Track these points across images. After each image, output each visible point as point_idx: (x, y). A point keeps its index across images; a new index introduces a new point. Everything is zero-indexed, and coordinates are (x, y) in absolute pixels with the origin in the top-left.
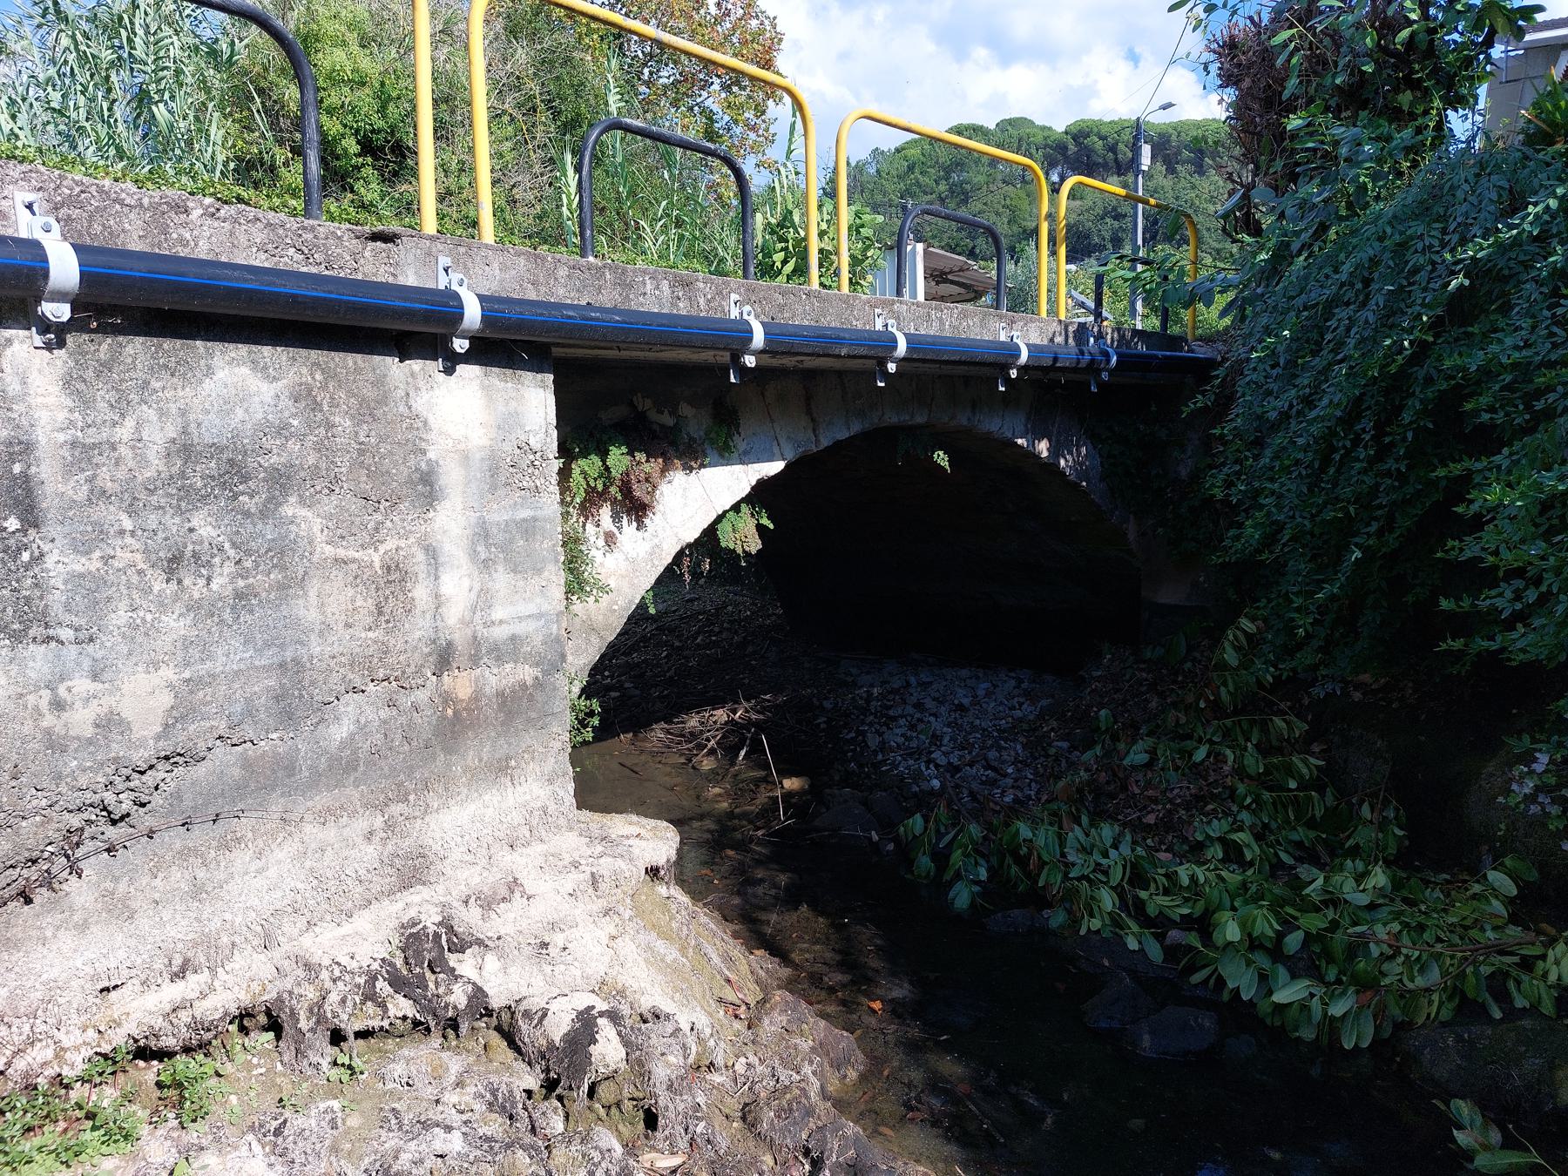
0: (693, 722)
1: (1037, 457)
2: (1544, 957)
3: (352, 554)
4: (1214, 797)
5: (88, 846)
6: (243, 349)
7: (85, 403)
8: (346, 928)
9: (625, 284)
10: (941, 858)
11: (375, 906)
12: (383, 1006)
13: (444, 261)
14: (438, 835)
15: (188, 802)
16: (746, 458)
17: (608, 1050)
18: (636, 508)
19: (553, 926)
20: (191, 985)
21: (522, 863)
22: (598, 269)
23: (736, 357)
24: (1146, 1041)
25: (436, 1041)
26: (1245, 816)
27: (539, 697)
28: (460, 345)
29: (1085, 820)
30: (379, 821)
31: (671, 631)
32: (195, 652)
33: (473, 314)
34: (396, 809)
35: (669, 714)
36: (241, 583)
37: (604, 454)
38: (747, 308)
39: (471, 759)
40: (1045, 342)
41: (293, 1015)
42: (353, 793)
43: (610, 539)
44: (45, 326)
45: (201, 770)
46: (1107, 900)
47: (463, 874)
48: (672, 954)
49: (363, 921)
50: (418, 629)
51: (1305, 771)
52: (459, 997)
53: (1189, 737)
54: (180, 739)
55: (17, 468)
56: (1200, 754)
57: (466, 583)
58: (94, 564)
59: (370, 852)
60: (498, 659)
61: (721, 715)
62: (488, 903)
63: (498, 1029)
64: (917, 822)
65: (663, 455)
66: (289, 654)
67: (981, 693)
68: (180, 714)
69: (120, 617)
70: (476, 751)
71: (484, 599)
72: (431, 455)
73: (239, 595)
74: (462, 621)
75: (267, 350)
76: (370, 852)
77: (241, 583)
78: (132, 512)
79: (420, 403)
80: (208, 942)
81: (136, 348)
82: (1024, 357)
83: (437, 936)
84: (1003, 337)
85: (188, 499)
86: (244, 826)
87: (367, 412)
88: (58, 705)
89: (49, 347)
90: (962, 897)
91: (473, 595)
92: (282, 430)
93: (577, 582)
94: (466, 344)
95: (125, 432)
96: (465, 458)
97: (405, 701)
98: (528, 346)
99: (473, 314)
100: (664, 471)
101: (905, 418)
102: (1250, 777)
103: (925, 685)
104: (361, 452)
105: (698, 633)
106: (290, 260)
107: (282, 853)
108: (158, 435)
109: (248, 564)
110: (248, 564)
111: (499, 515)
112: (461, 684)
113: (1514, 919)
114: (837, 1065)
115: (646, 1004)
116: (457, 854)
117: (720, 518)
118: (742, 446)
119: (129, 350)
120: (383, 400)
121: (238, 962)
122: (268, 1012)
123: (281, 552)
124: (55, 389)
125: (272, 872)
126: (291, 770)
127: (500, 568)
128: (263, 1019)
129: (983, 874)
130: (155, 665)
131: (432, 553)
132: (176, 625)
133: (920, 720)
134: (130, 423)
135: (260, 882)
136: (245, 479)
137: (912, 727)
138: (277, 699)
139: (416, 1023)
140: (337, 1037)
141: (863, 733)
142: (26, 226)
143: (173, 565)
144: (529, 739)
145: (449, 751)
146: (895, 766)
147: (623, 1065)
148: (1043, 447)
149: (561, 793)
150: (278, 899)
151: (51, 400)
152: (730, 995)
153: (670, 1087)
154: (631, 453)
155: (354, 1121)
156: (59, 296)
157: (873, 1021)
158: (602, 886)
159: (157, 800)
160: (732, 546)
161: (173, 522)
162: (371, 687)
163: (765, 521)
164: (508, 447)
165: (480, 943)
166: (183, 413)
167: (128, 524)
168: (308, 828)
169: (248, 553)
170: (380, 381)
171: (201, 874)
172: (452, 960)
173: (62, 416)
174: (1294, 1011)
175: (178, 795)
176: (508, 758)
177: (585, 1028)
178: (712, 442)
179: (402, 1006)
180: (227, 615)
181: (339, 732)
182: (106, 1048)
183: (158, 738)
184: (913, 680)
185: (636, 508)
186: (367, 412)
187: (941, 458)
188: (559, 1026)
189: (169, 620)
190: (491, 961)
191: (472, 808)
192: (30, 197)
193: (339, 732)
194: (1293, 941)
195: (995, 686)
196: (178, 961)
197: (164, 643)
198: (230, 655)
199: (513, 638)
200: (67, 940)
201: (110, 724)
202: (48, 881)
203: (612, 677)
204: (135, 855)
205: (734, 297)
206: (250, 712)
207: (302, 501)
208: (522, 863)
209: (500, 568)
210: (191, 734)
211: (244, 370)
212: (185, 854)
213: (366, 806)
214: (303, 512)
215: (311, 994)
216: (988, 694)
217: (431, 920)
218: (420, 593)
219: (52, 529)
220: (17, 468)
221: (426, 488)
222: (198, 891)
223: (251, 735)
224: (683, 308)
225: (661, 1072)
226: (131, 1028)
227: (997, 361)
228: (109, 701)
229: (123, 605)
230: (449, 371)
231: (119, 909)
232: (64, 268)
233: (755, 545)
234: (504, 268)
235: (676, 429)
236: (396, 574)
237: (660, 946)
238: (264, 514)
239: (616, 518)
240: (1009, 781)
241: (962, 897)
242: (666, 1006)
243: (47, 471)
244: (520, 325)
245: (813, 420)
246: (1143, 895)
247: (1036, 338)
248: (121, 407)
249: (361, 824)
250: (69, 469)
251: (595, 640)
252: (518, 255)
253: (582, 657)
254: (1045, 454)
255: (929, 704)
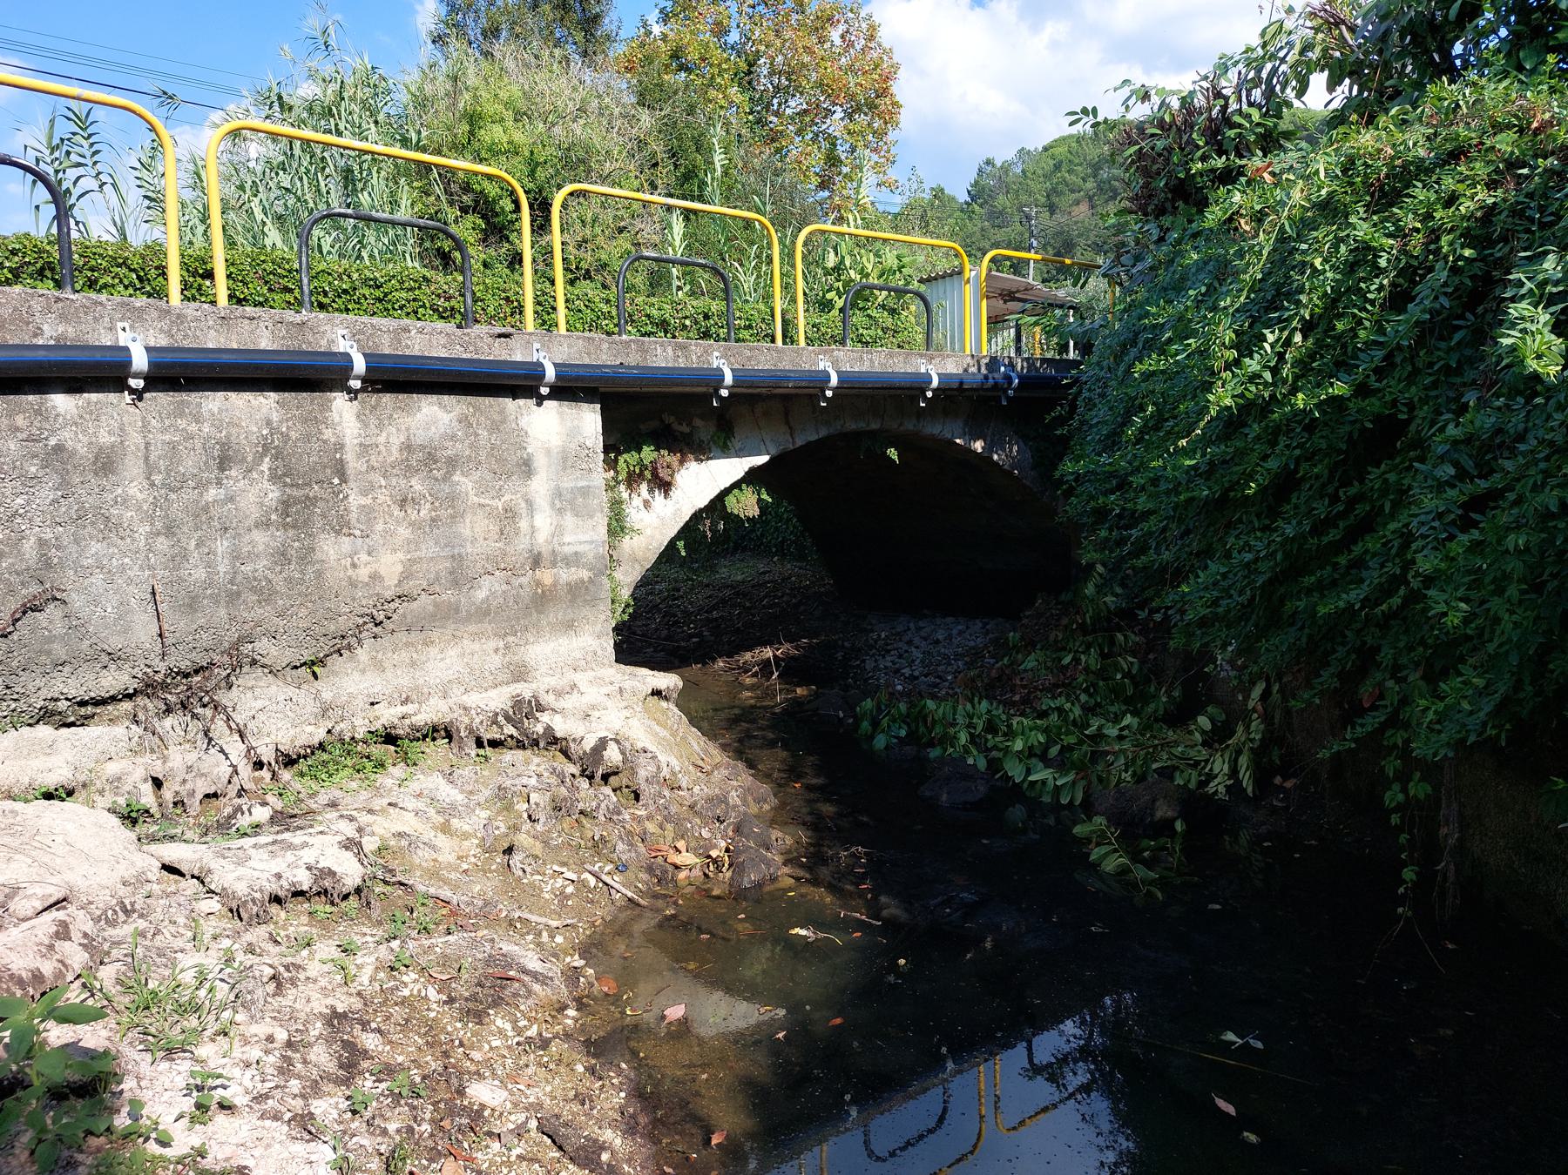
0: (748, 656)
1: (975, 452)
2: (1207, 761)
3: (487, 502)
4: (1064, 685)
5: (365, 634)
6: (435, 397)
7: (366, 425)
8: (484, 695)
9: (643, 350)
10: (875, 724)
11: (499, 688)
12: (501, 727)
13: (537, 345)
14: (533, 657)
15: (409, 620)
16: (726, 451)
17: (613, 755)
18: (664, 486)
19: (593, 707)
20: (409, 709)
21: (581, 678)
22: (626, 342)
23: (717, 390)
24: (944, 797)
25: (528, 752)
26: (1084, 698)
27: (592, 588)
28: (544, 391)
29: (976, 699)
30: (501, 644)
31: (745, 595)
32: (412, 546)
33: (550, 374)
34: (510, 639)
35: (732, 651)
36: (434, 514)
37: (639, 451)
38: (723, 361)
39: (551, 617)
40: (961, 371)
41: (458, 730)
42: (488, 627)
43: (647, 504)
44: (350, 391)
45: (415, 605)
46: (963, 738)
47: (548, 679)
48: (664, 733)
49: (493, 693)
50: (522, 544)
51: (1125, 666)
52: (540, 729)
53: (1064, 649)
54: (404, 589)
55: (338, 456)
56: (1067, 660)
57: (549, 520)
58: (369, 501)
59: (497, 660)
60: (567, 564)
61: (768, 653)
62: (559, 694)
63: (561, 751)
64: (868, 704)
65: (680, 451)
66: (456, 552)
67: (955, 632)
68: (406, 576)
69: (379, 527)
70: (555, 614)
71: (559, 530)
72: (529, 450)
73: (433, 520)
74: (546, 541)
75: (446, 397)
76: (497, 660)
77: (434, 514)
78: (385, 477)
79: (523, 422)
80: (416, 688)
81: (387, 399)
82: (935, 383)
83: (530, 702)
84: (923, 370)
85: (410, 471)
86: (435, 635)
87: (495, 427)
88: (354, 566)
89: (351, 400)
90: (880, 742)
91: (553, 527)
92: (453, 437)
93: (617, 526)
94: (548, 390)
95: (382, 439)
96: (548, 452)
97: (516, 582)
98: (584, 389)
99: (550, 374)
100: (682, 462)
101: (862, 425)
102: (1092, 672)
103: (919, 629)
104: (492, 449)
105: (765, 597)
106: (458, 352)
107: (452, 652)
108: (397, 440)
109: (437, 504)
110: (437, 504)
111: (568, 483)
112: (546, 576)
113: (1204, 744)
114: (758, 801)
115: (639, 745)
116: (543, 669)
117: (726, 492)
118: (738, 445)
119: (384, 400)
120: (504, 421)
121: (432, 701)
122: (446, 729)
123: (452, 499)
124: (354, 419)
125: (448, 661)
126: (457, 611)
127: (568, 514)
128: (443, 733)
129: (903, 733)
130: (395, 551)
131: (530, 503)
132: (404, 532)
133: (906, 651)
134: (384, 434)
135: (441, 665)
136: (436, 462)
137: (900, 656)
138: (451, 573)
139: (518, 741)
140: (479, 743)
141: (864, 661)
142: (342, 346)
143: (403, 503)
144: (586, 611)
145: (540, 612)
146: (878, 680)
147: (621, 764)
148: (978, 446)
149: (605, 645)
150: (450, 675)
151: (351, 424)
152: (700, 763)
153: (647, 780)
154: (657, 449)
155: (486, 773)
156: (357, 378)
157: (793, 791)
158: (625, 694)
159: (395, 617)
160: (736, 512)
161: (403, 482)
162: (497, 573)
163: (765, 496)
164: (572, 446)
165: (553, 710)
166: (408, 429)
167: (383, 483)
168: (465, 642)
169: (437, 499)
170: (502, 412)
171: (415, 655)
172: (538, 714)
173: (356, 431)
174: (1039, 785)
175: (404, 616)
176: (573, 620)
177: (602, 744)
178: (715, 443)
179: (510, 730)
180: (427, 529)
181: (481, 594)
182: (373, 729)
183: (396, 586)
184: (912, 625)
185: (664, 486)
186: (495, 427)
187: (893, 453)
188: (588, 745)
189: (401, 530)
190: (558, 718)
191: (552, 645)
192: (345, 332)
193: (481, 594)
194: (1054, 751)
195: (968, 628)
196: (404, 696)
197: (398, 541)
198: (429, 549)
199: (576, 553)
200: (356, 676)
201: (375, 577)
202: (349, 647)
203: (695, 628)
204: (385, 641)
205: (716, 354)
206: (438, 579)
207: (463, 474)
208: (581, 678)
209: (568, 514)
210: (410, 586)
211: (436, 408)
212: (407, 644)
213: (495, 635)
214: (463, 479)
215: (467, 721)
216: (960, 633)
217: (527, 695)
218: (523, 524)
219: (352, 484)
220: (338, 456)
221: (526, 468)
222: (413, 664)
223: (438, 590)
224: (682, 363)
225: (642, 774)
226: (383, 721)
227: (916, 386)
228: (375, 566)
229: (381, 521)
230: (539, 404)
231: (379, 666)
232: (360, 365)
233: (754, 511)
234: (570, 346)
235: (690, 434)
236: (510, 514)
237: (658, 729)
238: (445, 479)
239: (651, 491)
240: (947, 684)
241: (880, 742)
242: (650, 747)
243: (350, 456)
244: (578, 378)
245: (790, 428)
246: (990, 737)
247: (952, 367)
248: (381, 427)
249: (492, 644)
250: (359, 456)
251: (637, 567)
252: (578, 338)
253: (627, 578)
254: (980, 450)
255: (917, 641)
